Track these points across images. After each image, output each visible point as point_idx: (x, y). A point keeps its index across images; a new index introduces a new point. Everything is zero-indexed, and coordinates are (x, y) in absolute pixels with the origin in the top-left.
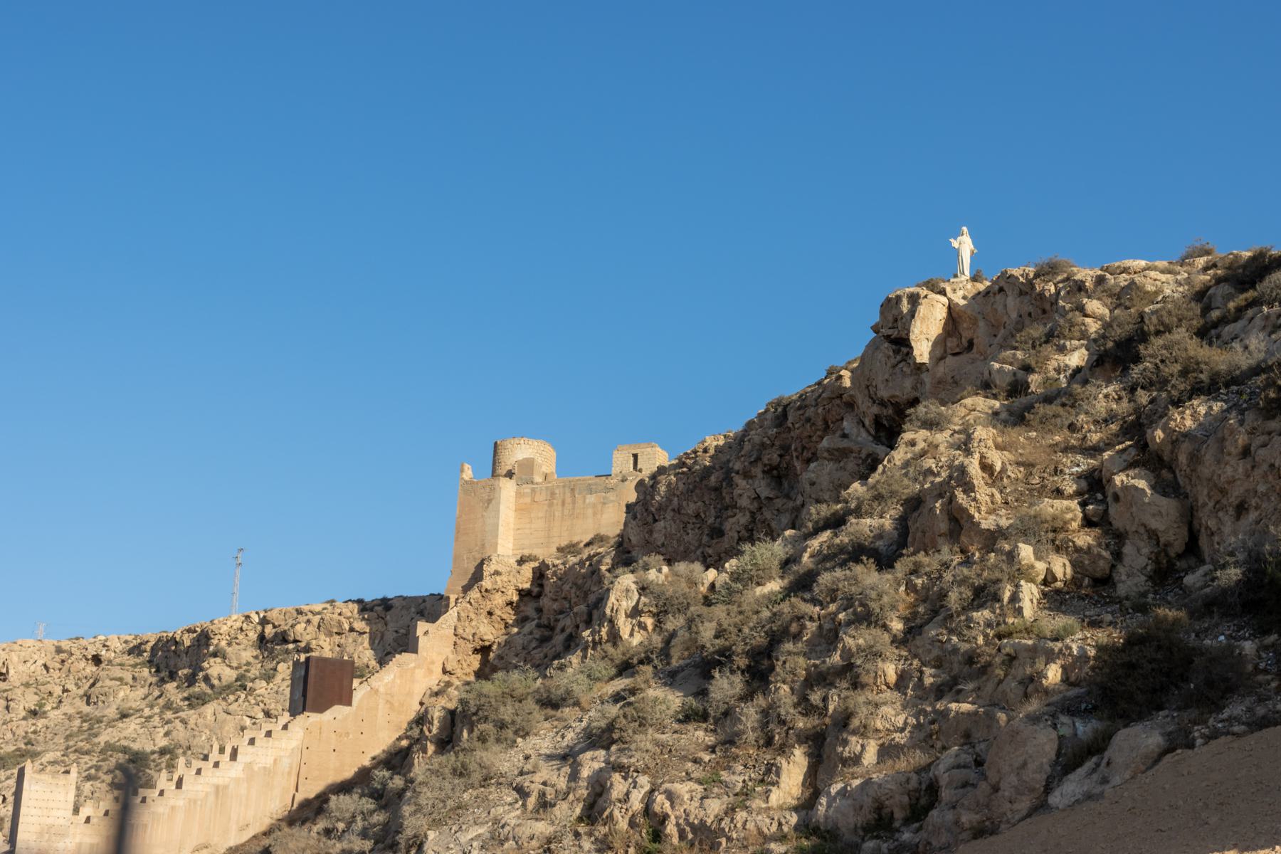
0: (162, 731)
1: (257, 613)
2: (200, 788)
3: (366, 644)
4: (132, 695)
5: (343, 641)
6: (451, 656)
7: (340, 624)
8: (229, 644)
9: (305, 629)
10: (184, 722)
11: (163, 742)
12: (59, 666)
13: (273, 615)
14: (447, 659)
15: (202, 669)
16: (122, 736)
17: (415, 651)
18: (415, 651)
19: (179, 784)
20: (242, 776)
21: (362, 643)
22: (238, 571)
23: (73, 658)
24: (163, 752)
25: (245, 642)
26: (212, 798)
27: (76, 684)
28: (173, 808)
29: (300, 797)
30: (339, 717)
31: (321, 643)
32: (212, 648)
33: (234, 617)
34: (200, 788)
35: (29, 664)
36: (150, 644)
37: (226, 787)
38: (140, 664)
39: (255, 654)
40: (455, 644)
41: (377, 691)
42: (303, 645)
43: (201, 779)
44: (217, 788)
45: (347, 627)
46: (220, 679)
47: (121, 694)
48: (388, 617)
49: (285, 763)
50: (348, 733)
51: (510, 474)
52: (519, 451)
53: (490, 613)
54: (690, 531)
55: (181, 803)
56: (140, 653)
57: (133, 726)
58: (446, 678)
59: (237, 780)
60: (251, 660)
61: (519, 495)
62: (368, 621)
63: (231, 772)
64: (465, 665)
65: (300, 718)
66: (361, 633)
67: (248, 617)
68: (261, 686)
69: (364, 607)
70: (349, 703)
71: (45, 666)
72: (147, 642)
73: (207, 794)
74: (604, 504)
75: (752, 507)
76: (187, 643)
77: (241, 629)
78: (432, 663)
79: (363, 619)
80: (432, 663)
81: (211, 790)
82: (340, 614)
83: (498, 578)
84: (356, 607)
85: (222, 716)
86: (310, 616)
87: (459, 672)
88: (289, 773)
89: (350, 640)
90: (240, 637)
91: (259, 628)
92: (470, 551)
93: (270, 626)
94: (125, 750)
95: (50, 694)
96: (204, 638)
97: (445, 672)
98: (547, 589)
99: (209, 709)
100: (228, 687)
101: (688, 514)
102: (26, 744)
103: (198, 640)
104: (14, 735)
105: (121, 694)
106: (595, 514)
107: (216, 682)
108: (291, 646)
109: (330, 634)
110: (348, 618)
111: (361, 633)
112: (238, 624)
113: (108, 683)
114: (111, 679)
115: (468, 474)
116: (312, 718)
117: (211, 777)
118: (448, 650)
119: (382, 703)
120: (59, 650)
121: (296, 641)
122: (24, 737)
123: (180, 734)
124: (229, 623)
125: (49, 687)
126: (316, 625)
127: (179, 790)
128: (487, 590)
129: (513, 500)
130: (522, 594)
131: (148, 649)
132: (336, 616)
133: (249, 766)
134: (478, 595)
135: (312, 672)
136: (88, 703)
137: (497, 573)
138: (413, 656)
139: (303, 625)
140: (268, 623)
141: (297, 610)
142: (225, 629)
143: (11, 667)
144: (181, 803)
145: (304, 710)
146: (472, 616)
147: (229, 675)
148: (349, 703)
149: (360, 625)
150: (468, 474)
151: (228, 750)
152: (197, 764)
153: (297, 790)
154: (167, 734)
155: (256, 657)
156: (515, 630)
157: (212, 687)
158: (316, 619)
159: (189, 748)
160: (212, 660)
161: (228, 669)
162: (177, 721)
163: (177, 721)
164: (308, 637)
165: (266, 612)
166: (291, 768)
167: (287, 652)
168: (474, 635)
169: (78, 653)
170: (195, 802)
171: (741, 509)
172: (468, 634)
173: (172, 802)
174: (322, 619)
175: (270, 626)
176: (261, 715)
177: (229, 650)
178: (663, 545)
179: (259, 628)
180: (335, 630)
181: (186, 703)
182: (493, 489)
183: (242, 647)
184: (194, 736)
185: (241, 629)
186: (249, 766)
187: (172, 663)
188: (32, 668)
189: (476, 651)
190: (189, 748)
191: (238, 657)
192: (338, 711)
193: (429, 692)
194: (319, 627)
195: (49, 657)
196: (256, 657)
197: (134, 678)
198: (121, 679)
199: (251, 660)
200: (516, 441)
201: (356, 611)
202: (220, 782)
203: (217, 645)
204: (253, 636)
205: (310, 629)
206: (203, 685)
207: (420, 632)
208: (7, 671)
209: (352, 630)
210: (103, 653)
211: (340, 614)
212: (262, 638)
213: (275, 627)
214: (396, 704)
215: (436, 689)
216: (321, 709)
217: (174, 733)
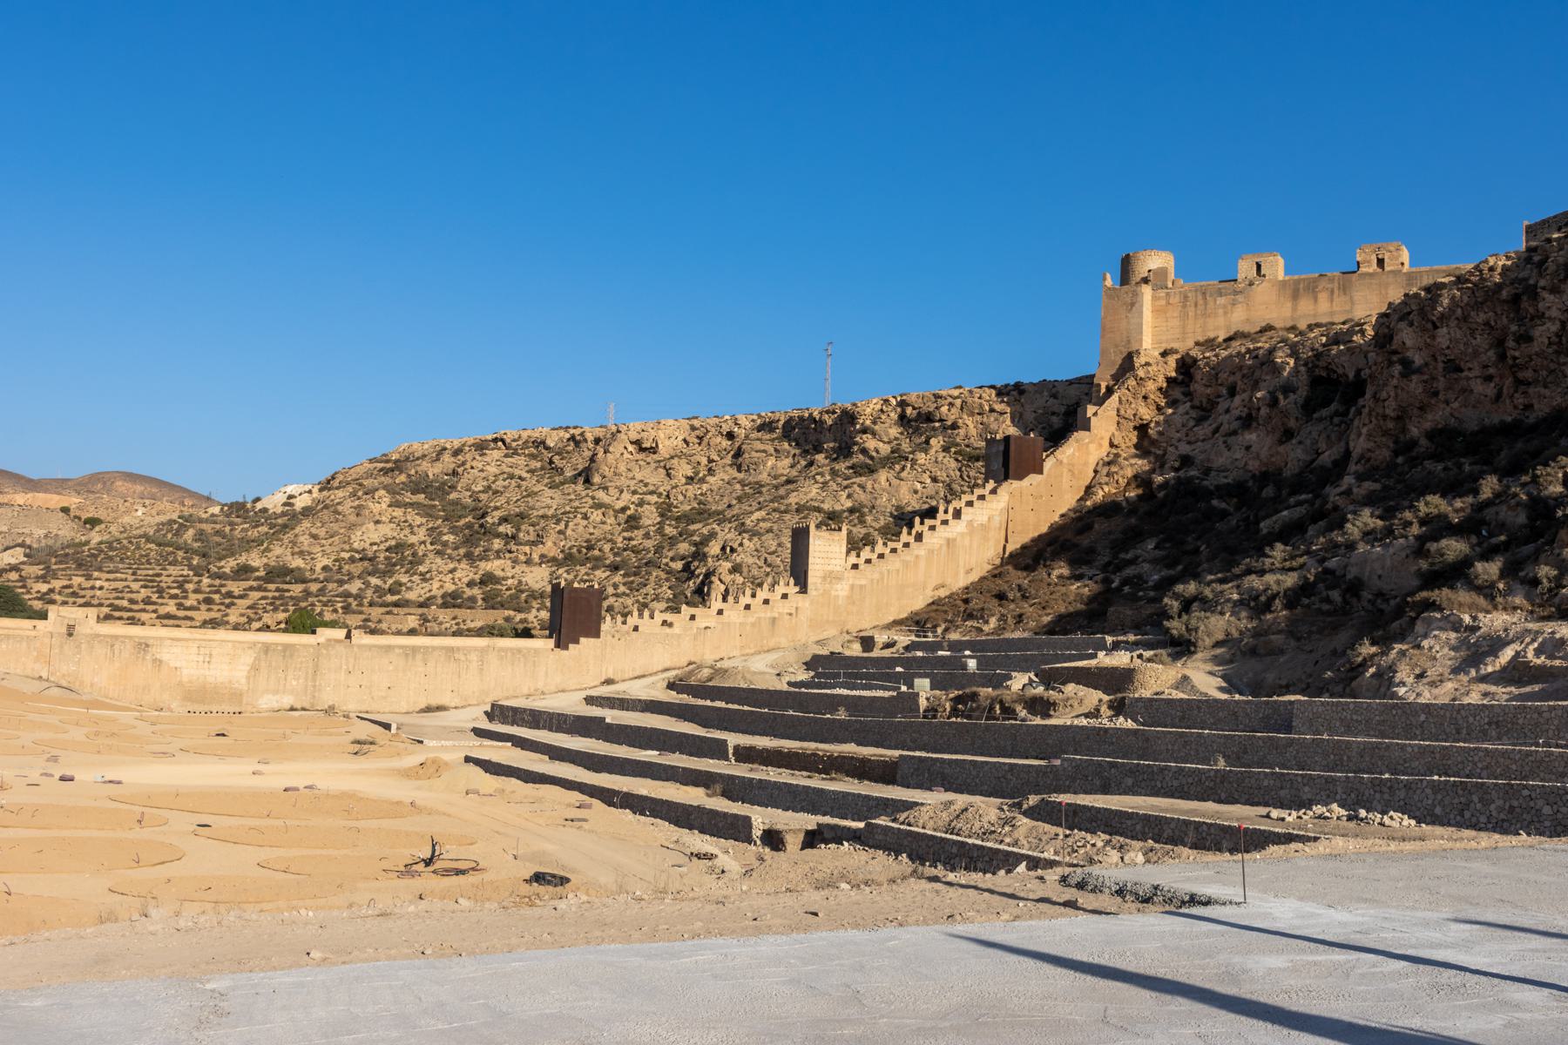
0: (844, 494)
1: (894, 397)
2: (935, 541)
3: (1008, 422)
4: (779, 464)
5: (985, 420)
6: (1116, 433)
7: (981, 406)
8: (874, 423)
9: (949, 410)
10: (862, 487)
11: (849, 504)
12: (697, 441)
13: (912, 398)
14: (1113, 435)
15: (856, 443)
16: (808, 498)
17: (1089, 430)
18: (1087, 428)
19: (919, 537)
20: (965, 531)
21: (1004, 422)
22: (829, 360)
23: (710, 434)
24: (852, 511)
25: (888, 421)
26: (944, 548)
27: (719, 455)
28: (917, 557)
29: (1011, 548)
30: (1034, 483)
31: (967, 422)
32: (858, 427)
33: (875, 401)
34: (935, 541)
35: (672, 440)
36: (781, 423)
37: (954, 540)
38: (776, 438)
39: (900, 431)
40: (1118, 423)
41: (1061, 462)
42: (949, 423)
43: (936, 534)
44: (948, 540)
45: (987, 408)
46: (877, 452)
47: (770, 463)
48: (1022, 400)
49: (997, 519)
50: (1042, 496)
51: (1146, 281)
52: (1154, 261)
53: (1145, 398)
54: (1478, 336)
55: (922, 552)
56: (772, 430)
57: (815, 491)
58: (1114, 451)
59: (962, 534)
60: (898, 435)
61: (1154, 298)
62: (1008, 404)
63: (957, 528)
64: (1127, 440)
65: (1005, 485)
66: (1002, 414)
67: (886, 401)
68: (921, 458)
69: (1001, 392)
70: (1041, 472)
71: (685, 440)
72: (778, 420)
73: (941, 545)
74: (1234, 305)
75: (1562, 318)
76: (830, 422)
77: (882, 410)
78: (1102, 438)
79: (1003, 402)
80: (1102, 438)
81: (943, 542)
82: (980, 398)
83: (1150, 368)
84: (994, 392)
85: (895, 482)
86: (950, 400)
87: (1123, 446)
88: (1000, 528)
89: (992, 419)
90: (883, 417)
91: (899, 409)
92: (1117, 346)
93: (910, 408)
94: (818, 510)
95: (699, 463)
96: (848, 417)
97: (1112, 445)
98: (1198, 377)
99: (883, 476)
100: (888, 458)
101: (1477, 323)
102: (698, 504)
103: (840, 418)
104: (685, 497)
105: (770, 463)
106: (1225, 313)
107: (874, 454)
108: (937, 424)
109: (972, 414)
110: (988, 401)
111: (1002, 414)
112: (879, 407)
113: (754, 454)
114: (757, 451)
115: (1109, 282)
116: (1013, 485)
117: (942, 532)
118: (1113, 428)
119: (1065, 470)
120: (693, 428)
121: (941, 420)
122: (695, 499)
123: (861, 496)
124: (872, 406)
125: (698, 458)
126: (959, 406)
127: (918, 543)
128: (1141, 379)
129: (1150, 302)
130: (1169, 380)
131: (780, 426)
132: (976, 400)
133: (970, 523)
134: (1134, 383)
135: (1012, 447)
136: (739, 471)
137: (1148, 364)
138: (1087, 433)
139: (947, 407)
140: (908, 405)
141: (934, 395)
142: (868, 411)
143: (659, 442)
144: (922, 552)
145: (1006, 478)
146: (1131, 399)
147: (885, 449)
148: (1041, 472)
149: (998, 407)
150: (1109, 282)
151: (951, 510)
152: (928, 522)
153: (1007, 541)
154: (849, 496)
155: (902, 433)
156: (1170, 411)
157: (872, 458)
158: (958, 402)
159: (873, 507)
160: (864, 436)
161: (881, 444)
162: (855, 486)
163: (855, 486)
164: (953, 417)
165: (901, 396)
166: (1001, 525)
167: (934, 429)
168: (1135, 415)
169: (713, 430)
170: (933, 551)
171: (1550, 318)
172: (1130, 413)
173: (916, 552)
174: (963, 402)
175: (910, 408)
176: (929, 481)
177: (876, 427)
178: (1448, 348)
179: (899, 409)
180: (977, 411)
181: (851, 471)
182: (1136, 294)
183: (886, 425)
184: (876, 498)
185: (882, 410)
186: (970, 523)
187: (812, 438)
188: (675, 443)
189: (1135, 428)
190: (873, 507)
191: (887, 434)
192: (1032, 479)
193: (1101, 462)
194: (962, 409)
195: (687, 433)
196: (902, 433)
197: (776, 450)
198: (764, 451)
199: (898, 435)
200: (1148, 252)
201: (993, 395)
202: (950, 535)
203: (862, 424)
204: (894, 416)
205: (953, 410)
206: (861, 456)
207: (1089, 414)
208: (657, 445)
209: (992, 410)
210: (736, 429)
211: (980, 398)
212: (902, 417)
213: (914, 408)
214: (1076, 472)
215: (1106, 459)
216: (1020, 478)
217: (855, 496)
